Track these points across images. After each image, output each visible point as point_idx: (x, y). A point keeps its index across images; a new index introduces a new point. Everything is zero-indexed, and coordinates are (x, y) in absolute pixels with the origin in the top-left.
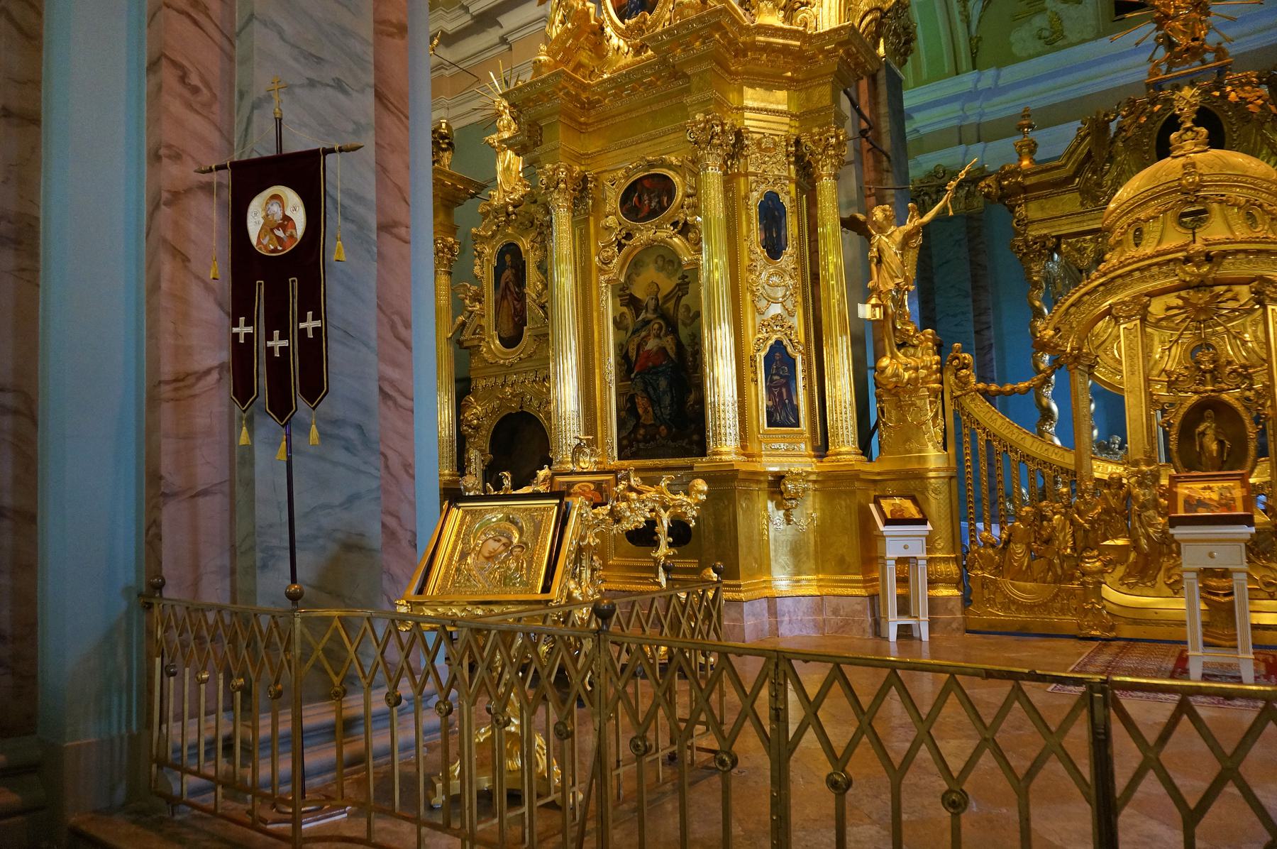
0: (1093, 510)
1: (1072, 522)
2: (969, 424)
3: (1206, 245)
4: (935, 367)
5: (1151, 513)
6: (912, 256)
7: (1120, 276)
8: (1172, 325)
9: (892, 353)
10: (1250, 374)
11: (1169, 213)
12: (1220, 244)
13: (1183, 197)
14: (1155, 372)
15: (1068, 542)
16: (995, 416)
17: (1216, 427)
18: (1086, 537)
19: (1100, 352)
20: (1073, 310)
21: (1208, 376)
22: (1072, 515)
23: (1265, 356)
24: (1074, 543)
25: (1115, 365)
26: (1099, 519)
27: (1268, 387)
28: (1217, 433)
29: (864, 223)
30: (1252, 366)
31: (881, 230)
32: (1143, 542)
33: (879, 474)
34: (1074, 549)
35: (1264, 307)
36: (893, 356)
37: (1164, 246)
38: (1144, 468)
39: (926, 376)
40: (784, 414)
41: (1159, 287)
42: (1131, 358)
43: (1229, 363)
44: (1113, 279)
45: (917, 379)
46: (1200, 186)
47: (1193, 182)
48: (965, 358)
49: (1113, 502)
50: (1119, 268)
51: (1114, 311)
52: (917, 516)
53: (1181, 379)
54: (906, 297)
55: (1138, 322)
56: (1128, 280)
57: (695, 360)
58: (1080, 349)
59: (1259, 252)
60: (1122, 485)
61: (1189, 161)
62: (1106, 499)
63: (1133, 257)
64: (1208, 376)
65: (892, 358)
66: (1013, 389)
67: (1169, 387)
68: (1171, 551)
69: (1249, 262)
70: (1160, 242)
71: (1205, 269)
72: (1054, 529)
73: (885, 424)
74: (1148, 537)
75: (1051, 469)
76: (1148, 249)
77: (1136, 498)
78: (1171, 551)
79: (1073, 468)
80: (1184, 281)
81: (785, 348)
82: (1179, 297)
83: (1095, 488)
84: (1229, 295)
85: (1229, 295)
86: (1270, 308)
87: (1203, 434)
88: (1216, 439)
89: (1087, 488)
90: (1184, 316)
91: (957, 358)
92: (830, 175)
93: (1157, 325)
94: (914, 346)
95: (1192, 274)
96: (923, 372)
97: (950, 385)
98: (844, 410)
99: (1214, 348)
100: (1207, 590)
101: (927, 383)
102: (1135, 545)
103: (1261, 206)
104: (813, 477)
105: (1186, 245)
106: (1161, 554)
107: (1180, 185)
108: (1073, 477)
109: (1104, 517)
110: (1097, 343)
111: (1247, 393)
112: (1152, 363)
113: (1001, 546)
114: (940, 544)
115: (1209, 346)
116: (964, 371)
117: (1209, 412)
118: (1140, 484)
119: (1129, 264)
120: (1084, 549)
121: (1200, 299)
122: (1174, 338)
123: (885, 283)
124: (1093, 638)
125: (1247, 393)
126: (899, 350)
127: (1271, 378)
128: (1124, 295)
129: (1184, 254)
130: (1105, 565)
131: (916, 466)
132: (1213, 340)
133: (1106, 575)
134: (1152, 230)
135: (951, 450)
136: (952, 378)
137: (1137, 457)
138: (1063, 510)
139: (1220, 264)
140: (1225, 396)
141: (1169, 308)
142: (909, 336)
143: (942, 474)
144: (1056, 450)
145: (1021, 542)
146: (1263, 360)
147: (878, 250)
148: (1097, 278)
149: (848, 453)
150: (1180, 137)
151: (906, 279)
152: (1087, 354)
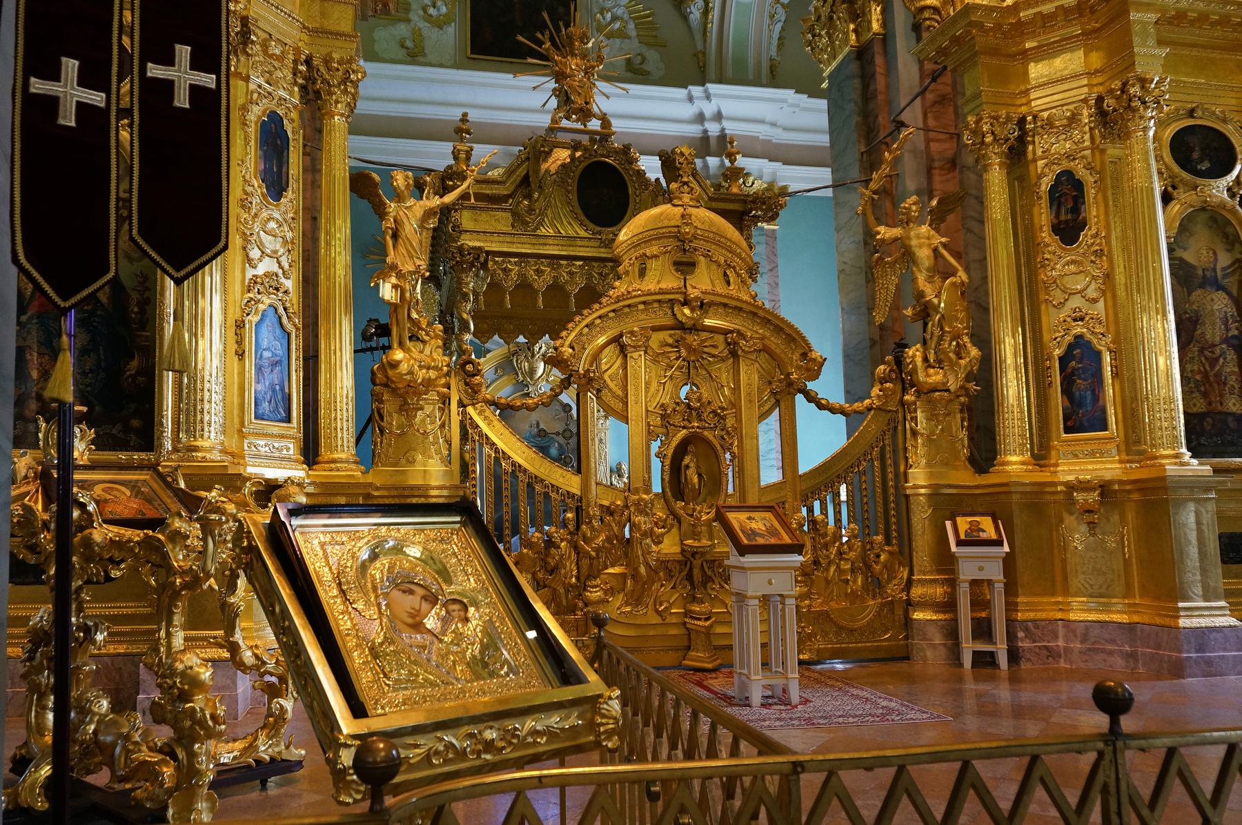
4: (445, 369)
5: (648, 541)
24: (578, 572)
27: (736, 429)
28: (698, 467)
34: (578, 578)
37: (663, 286)
55: (642, 353)
57: (143, 311)
70: (659, 282)
76: (650, 284)
87: (687, 467)
94: (424, 342)
98: (345, 407)
103: (734, 268)
117: (691, 448)
120: (589, 577)
140: (706, 433)
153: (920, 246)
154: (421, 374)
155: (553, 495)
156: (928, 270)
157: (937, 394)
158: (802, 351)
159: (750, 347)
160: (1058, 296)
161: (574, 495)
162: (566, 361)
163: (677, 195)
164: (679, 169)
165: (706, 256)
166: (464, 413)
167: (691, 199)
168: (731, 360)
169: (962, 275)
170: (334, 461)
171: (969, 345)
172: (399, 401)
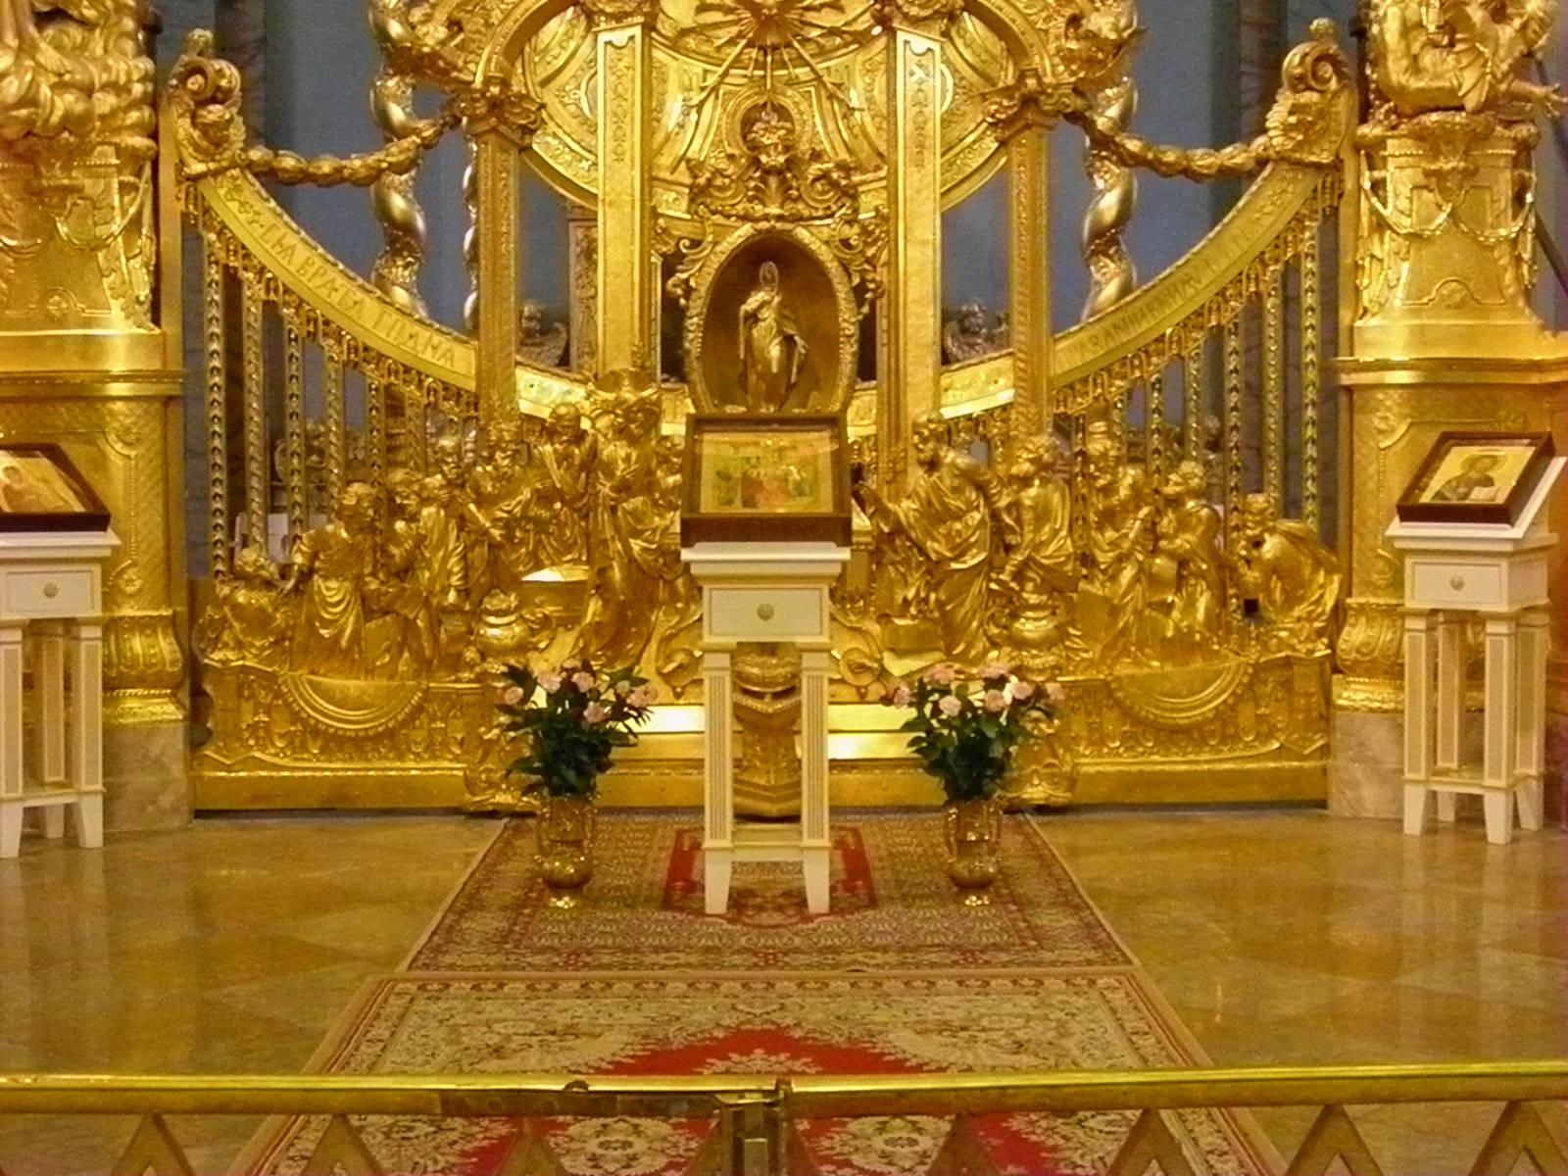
1: (463, 522)
2: (222, 255)
4: (138, 89)
5: (636, 502)
8: (705, 48)
9: (20, 34)
10: (855, 186)
14: (665, 160)
15: (450, 574)
17: (782, 304)
19: (548, 97)
21: (773, 181)
22: (464, 505)
23: (883, 148)
24: (465, 577)
25: (582, 133)
26: (524, 516)
27: (886, 219)
28: (781, 318)
30: (860, 168)
32: (617, 574)
34: (464, 593)
35: (890, 32)
39: (113, 113)
42: (618, 119)
43: (817, 156)
49: (558, 475)
52: (78, 508)
55: (637, 31)
58: (505, 83)
60: (579, 437)
64: (773, 181)
66: (339, 170)
67: (692, 200)
68: (674, 596)
72: (420, 540)
74: (630, 560)
77: (609, 470)
79: (471, 385)
86: (901, 36)
87: (753, 317)
88: (780, 332)
89: (500, 439)
90: (735, 30)
91: (200, 71)
93: (676, 44)
94: (83, 22)
96: (105, 102)
97: (178, 144)
100: (742, 684)
101: (118, 130)
102: (602, 585)
106: (653, 603)
109: (535, 511)
110: (542, 74)
112: (660, 137)
114: (133, 581)
115: (782, 112)
116: (216, 108)
117: (769, 269)
118: (621, 432)
120: (488, 592)
122: (711, 80)
124: (494, 814)
127: (893, 199)
130: (533, 632)
131: (76, 365)
132: (789, 99)
133: (533, 656)
135: (171, 326)
136: (184, 127)
137: (616, 367)
140: (803, 234)
146: (880, 155)
154: (67, 102)
155: (411, 390)
157: (1435, 117)
158: (1068, 12)
162: (434, 56)
166: (198, 199)
168: (882, 42)
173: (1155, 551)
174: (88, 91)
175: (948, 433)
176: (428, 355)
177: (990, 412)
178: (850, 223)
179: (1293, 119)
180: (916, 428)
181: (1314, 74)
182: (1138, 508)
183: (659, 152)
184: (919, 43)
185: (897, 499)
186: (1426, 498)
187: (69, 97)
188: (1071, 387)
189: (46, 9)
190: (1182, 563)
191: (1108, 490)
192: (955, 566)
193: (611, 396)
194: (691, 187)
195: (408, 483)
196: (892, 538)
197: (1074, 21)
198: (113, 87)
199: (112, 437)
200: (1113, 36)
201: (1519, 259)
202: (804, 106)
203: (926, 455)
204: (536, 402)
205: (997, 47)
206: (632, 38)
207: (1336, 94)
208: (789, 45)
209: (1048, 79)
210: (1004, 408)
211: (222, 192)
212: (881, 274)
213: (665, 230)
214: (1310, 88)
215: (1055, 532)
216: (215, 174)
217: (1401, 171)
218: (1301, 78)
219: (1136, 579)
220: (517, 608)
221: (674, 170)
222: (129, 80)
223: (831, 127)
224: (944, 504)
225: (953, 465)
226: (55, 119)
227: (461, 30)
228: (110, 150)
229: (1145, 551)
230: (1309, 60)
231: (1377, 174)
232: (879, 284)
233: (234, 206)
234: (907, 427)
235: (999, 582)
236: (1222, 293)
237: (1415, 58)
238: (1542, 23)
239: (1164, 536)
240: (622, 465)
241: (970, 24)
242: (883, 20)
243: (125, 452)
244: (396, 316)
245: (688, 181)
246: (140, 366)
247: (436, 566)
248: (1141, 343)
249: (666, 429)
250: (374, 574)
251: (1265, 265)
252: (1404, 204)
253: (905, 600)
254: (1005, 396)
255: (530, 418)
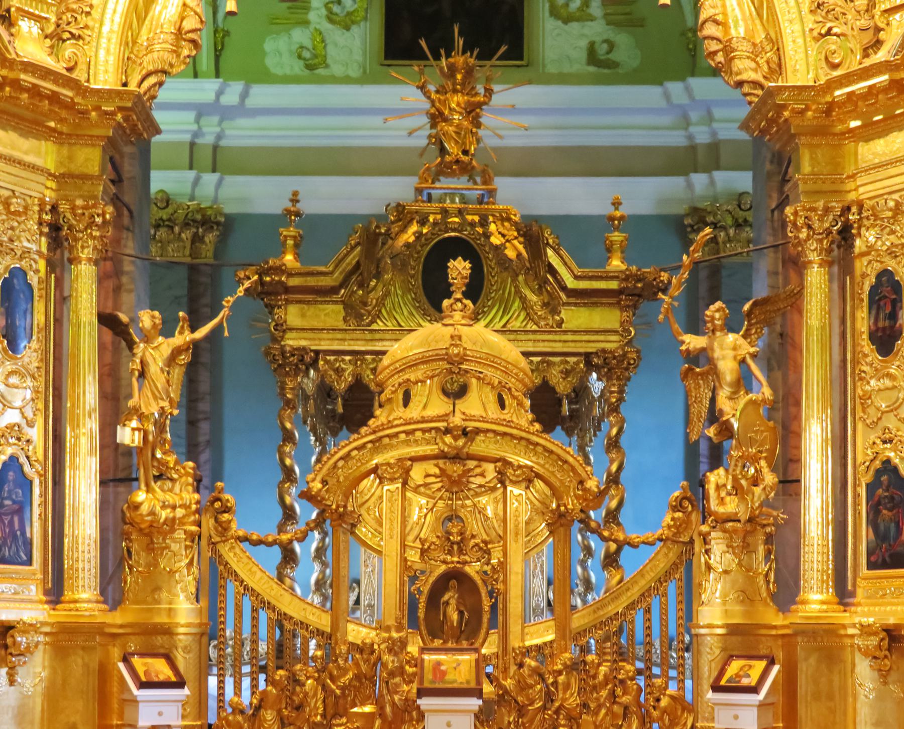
0: (344, 675)
1: (324, 687)
3: (464, 420)
4: (194, 507)
5: (397, 680)
6: (178, 374)
7: (388, 436)
8: (428, 492)
9: (147, 485)
11: (435, 379)
12: (475, 421)
13: (448, 366)
14: (411, 538)
15: (318, 709)
16: (255, 569)
17: (459, 598)
18: (336, 704)
19: (363, 511)
20: (341, 463)
21: (455, 547)
22: (324, 680)
23: (501, 534)
24: (325, 710)
25: (376, 526)
28: (458, 603)
29: (126, 326)
30: (491, 542)
31: (147, 339)
32: (388, 709)
33: (121, 626)
34: (324, 716)
35: (505, 487)
36: (149, 489)
37: (430, 412)
38: (395, 635)
39: (184, 516)
40: (14, 548)
41: (421, 453)
43: (473, 536)
44: (381, 438)
45: (174, 519)
46: (463, 359)
47: (458, 354)
48: (228, 501)
49: (364, 668)
50: (388, 428)
51: (379, 472)
53: (432, 547)
54: (168, 422)
55: (400, 485)
56: (394, 441)
58: (345, 507)
59: (504, 434)
61: (456, 333)
62: (357, 664)
63: (401, 418)
64: (455, 547)
65: (147, 492)
68: (412, 719)
69: (496, 442)
70: (425, 407)
71: (461, 442)
72: (306, 694)
73: (131, 568)
74: (394, 704)
75: (307, 630)
76: (414, 411)
77: (385, 665)
78: (412, 719)
79: (328, 630)
80: (443, 451)
81: (21, 466)
82: (437, 465)
83: (348, 652)
84: (478, 470)
85: (478, 470)
86: (509, 488)
87: (447, 603)
88: (458, 609)
89: (341, 652)
91: (219, 499)
92: (89, 260)
93: (416, 490)
94: (172, 480)
95: (449, 446)
96: (180, 512)
97: (209, 528)
99: (463, 521)
101: (184, 524)
102: (381, 713)
104: (47, 629)
105: (447, 415)
107: (447, 354)
108: (328, 639)
110: (360, 501)
111: (486, 568)
112: (408, 528)
113: (251, 712)
115: (458, 517)
116: (226, 515)
117: (453, 583)
118: (390, 650)
119: (397, 426)
120: (334, 716)
121: (455, 472)
122: (430, 506)
123: (148, 404)
125: (486, 568)
126: (155, 482)
127: (505, 554)
128: (390, 456)
129: (445, 424)
134: (419, 394)
135: (204, 603)
138: (316, 675)
139: (472, 440)
140: (467, 569)
141: (427, 476)
142: (168, 468)
143: (193, 630)
144: (315, 610)
145: (272, 708)
146: (500, 536)
147: (142, 362)
148: (366, 435)
149: (89, 601)
150: (451, 305)
151: (171, 401)
152: (351, 512)
153: (724, 358)
154: (164, 514)
156: (731, 385)
157: (730, 524)
158: (579, 479)
159: (518, 476)
160: (873, 414)
161: (323, 633)
163: (448, 313)
164: (451, 285)
165: (479, 379)
166: (215, 551)
167: (463, 317)
168: (501, 490)
169: (767, 392)
170: (76, 601)
171: (765, 470)
172: (146, 540)
173: (614, 702)
174: (174, 508)
175: (528, 651)
176: (311, 617)
177: (545, 644)
178: (487, 564)
179: (672, 523)
180: (514, 649)
181: (681, 505)
182: (607, 684)
183: (408, 534)
184: (517, 491)
185: (505, 680)
186: (723, 683)
187: (169, 510)
188: (579, 633)
189: (157, 474)
190: (626, 708)
191: (594, 677)
192: (530, 708)
193: (386, 635)
194: (421, 549)
195: (301, 670)
196: (503, 697)
197: (581, 482)
198: (183, 506)
199: (180, 650)
200: (596, 490)
201: (768, 582)
202: (468, 516)
203: (518, 661)
204: (355, 638)
205: (548, 491)
206: (397, 488)
207: (691, 513)
208: (462, 491)
209: (570, 507)
210: (551, 642)
211: (227, 549)
212: (500, 586)
213: (410, 567)
214: (679, 511)
215: (572, 694)
216: (224, 542)
217: (718, 546)
218: (675, 506)
219: (606, 714)
220: (346, 723)
221: (414, 541)
222: (190, 503)
223: (480, 524)
224: (525, 682)
225: (530, 666)
226: (162, 520)
227: (327, 484)
228: (182, 532)
229: (610, 703)
230: (679, 499)
231: (707, 547)
232: (498, 590)
233: (232, 555)
234: (510, 649)
235: (548, 715)
236: (643, 595)
237: (722, 499)
238: (771, 488)
239: (618, 696)
240: (390, 664)
241: (539, 484)
242: (502, 482)
243: (185, 655)
244: (298, 601)
245: (420, 546)
246: (191, 621)
247: (312, 705)
248: (609, 615)
249: (409, 649)
250: (286, 708)
251: (661, 584)
252: (718, 559)
253: (509, 722)
254: (550, 637)
255: (352, 644)
